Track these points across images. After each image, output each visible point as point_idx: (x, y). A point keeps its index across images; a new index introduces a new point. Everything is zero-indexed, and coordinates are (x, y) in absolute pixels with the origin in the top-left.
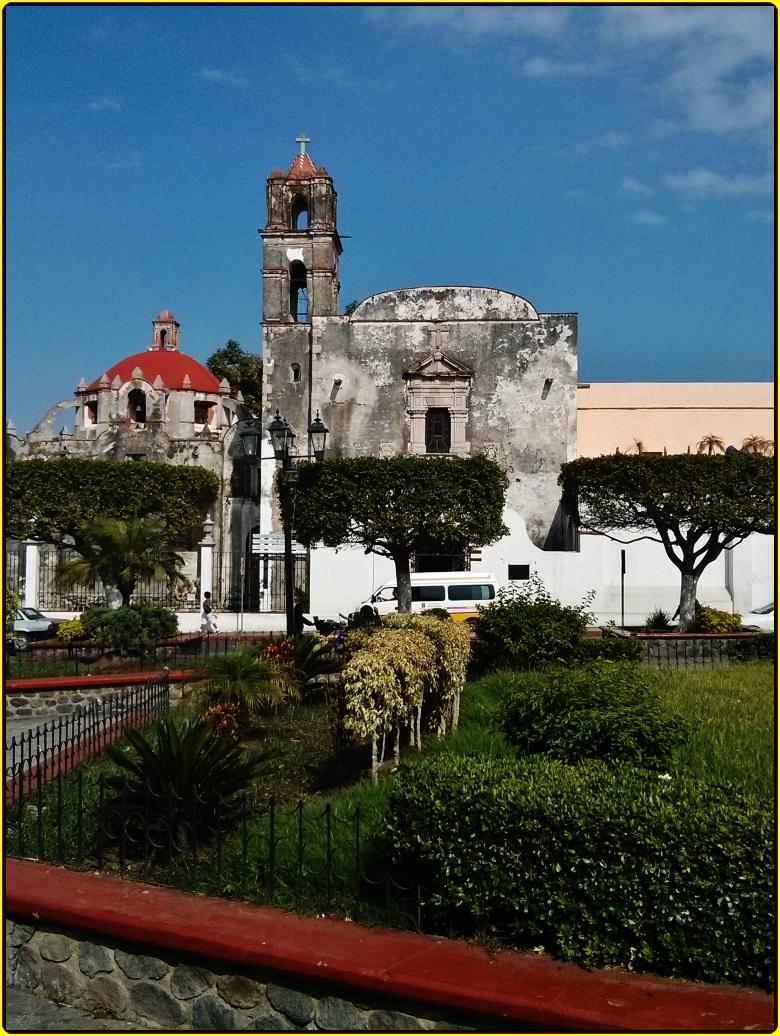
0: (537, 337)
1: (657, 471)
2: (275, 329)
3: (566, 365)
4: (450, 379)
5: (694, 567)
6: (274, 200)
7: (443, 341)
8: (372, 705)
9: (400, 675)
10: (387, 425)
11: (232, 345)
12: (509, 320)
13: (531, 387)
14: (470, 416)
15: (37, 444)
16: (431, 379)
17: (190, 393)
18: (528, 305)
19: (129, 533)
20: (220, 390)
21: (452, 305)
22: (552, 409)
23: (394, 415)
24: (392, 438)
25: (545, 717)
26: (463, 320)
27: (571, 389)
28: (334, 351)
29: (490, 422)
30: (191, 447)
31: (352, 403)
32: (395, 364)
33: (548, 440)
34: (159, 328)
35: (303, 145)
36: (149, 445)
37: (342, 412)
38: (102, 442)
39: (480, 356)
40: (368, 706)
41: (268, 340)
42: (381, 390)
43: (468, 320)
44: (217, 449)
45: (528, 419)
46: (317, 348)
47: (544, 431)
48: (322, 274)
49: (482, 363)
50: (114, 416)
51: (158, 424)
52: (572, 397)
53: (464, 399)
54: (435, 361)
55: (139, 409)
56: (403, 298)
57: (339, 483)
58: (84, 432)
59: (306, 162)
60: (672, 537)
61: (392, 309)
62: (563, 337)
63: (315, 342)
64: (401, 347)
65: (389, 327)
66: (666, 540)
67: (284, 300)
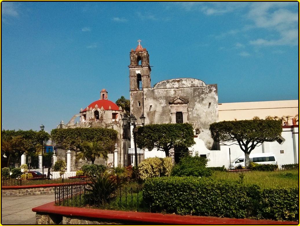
0: (206, 91)
1: (235, 125)
2: (133, 92)
3: (215, 99)
4: (182, 104)
5: (248, 151)
6: (132, 58)
7: (180, 93)
8: (145, 172)
9: (152, 166)
10: (165, 117)
11: (122, 97)
12: (198, 87)
13: (205, 105)
14: (188, 114)
15: (70, 126)
16: (177, 104)
17: (111, 111)
18: (203, 82)
19: (93, 145)
20: (119, 110)
21: (182, 84)
22: (211, 111)
23: (167, 114)
24: (167, 121)
25: (180, 171)
26: (185, 87)
27: (216, 105)
28: (149, 97)
29: (194, 115)
30: (111, 126)
31: (155, 111)
32: (166, 100)
33: (210, 119)
34: (102, 94)
35: (139, 42)
36: (100, 125)
37: (152, 114)
38: (87, 125)
39: (190, 97)
40: (144, 173)
41: (131, 95)
42: (163, 107)
43: (186, 87)
44: (119, 126)
45: (205, 114)
46: (145, 97)
47: (209, 117)
48: (146, 77)
49: (191, 99)
50: (90, 118)
51: (103, 120)
52: (217, 107)
53: (186, 109)
54: (178, 99)
55: (97, 116)
56: (168, 82)
57: (149, 131)
58: (82, 123)
59: (141, 47)
60: (242, 144)
61: (165, 85)
62: (213, 91)
63: (144, 95)
64: (168, 95)
65: (164, 90)
66: (240, 144)
67: (136, 84)
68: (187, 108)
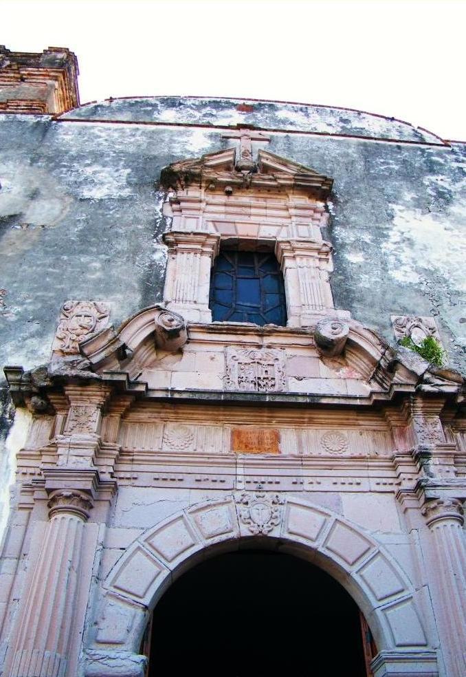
10: (97, 265)
23: (123, 245)
68: (324, 221)
